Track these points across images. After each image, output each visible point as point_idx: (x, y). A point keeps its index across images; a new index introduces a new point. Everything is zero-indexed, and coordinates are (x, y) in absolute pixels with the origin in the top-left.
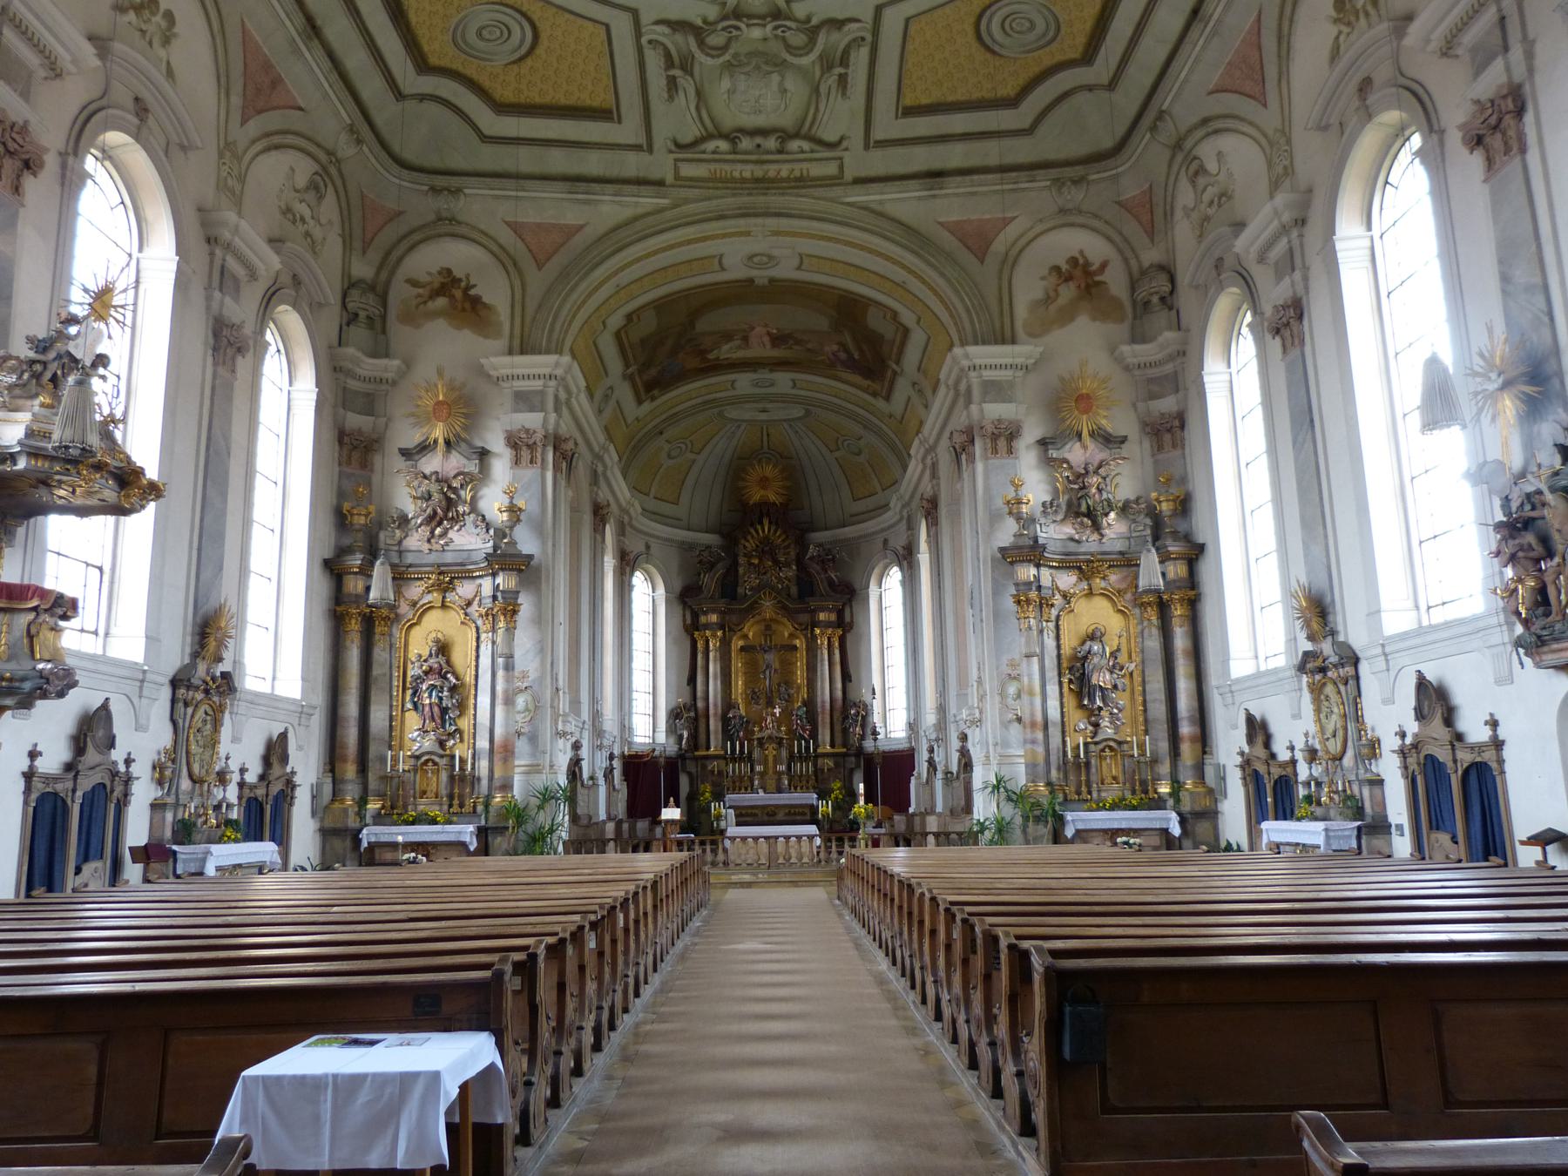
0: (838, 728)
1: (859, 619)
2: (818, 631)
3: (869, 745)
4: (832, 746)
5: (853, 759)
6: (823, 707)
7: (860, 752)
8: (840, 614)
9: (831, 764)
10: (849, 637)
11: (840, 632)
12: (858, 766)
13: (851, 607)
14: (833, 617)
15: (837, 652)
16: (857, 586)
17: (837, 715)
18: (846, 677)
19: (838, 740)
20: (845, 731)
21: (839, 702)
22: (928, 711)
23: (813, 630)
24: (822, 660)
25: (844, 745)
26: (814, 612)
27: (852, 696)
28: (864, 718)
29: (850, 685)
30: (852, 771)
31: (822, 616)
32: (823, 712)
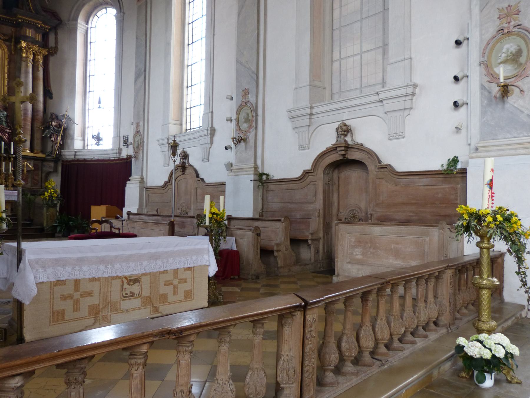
0: (38, 135)
1: (63, 46)
2: (24, 44)
3: (68, 154)
4: (32, 150)
5: (52, 164)
6: (26, 114)
7: (58, 158)
8: (45, 36)
9: (31, 167)
10: (52, 59)
11: (44, 52)
12: (56, 171)
13: (56, 34)
14: (39, 38)
15: (41, 69)
16: (64, 16)
17: (38, 124)
18: (48, 94)
19: (38, 145)
20: (44, 140)
21: (41, 114)
22: (171, 121)
23: (18, 42)
24: (27, 72)
25: (43, 152)
26: (19, 26)
27: (51, 109)
28: (65, 130)
29: (50, 101)
30: (48, 174)
31: (29, 33)
32: (25, 119)
